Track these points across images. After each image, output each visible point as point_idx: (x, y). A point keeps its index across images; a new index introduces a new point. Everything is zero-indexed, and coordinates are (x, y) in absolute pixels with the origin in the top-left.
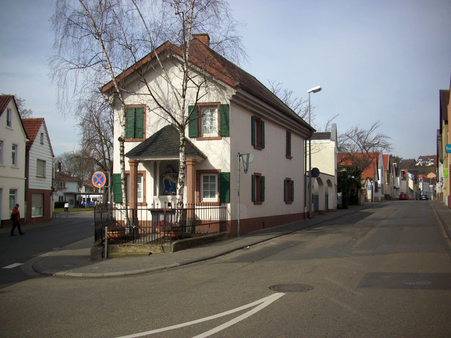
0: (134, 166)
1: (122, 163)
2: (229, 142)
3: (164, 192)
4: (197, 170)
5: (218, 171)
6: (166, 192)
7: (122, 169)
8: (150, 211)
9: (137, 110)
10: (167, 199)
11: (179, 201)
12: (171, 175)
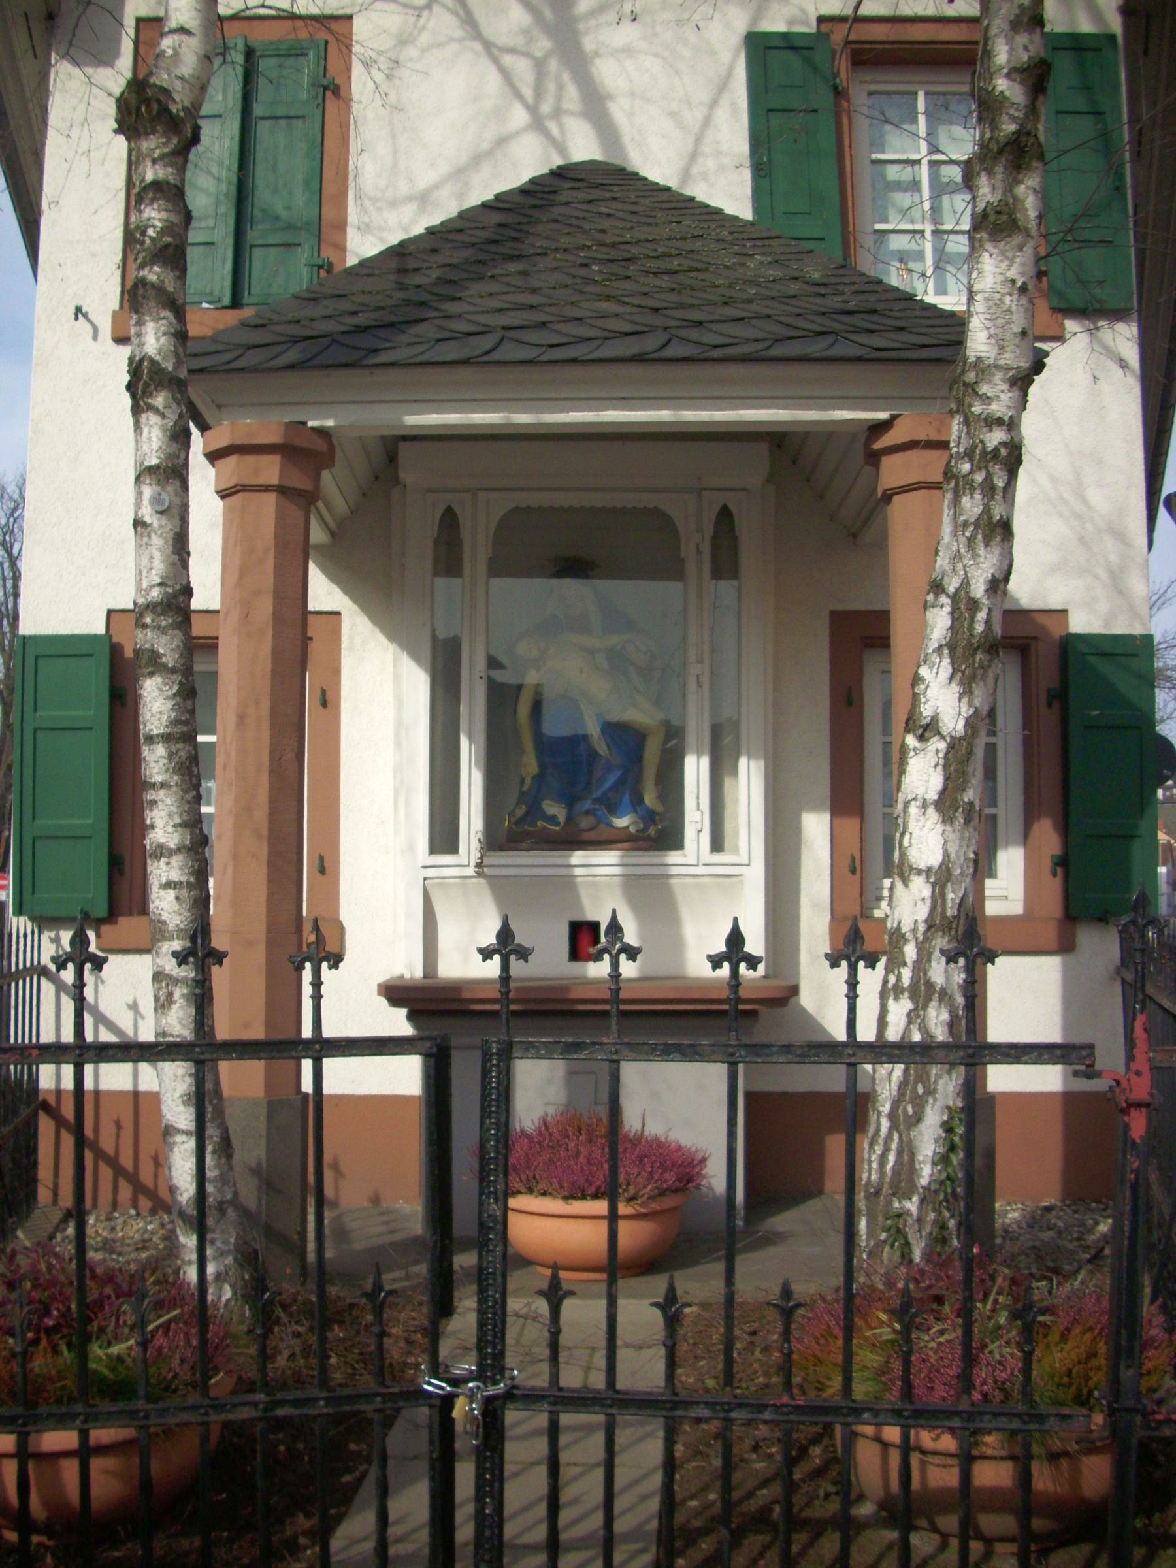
0: (270, 500)
1: (159, 400)
2: (1132, 354)
3: (534, 811)
4: (840, 607)
5: (1043, 627)
6: (552, 819)
7: (144, 473)
8: (404, 1012)
9: (266, 65)
10: (567, 884)
11: (937, 899)
12: (591, 652)
